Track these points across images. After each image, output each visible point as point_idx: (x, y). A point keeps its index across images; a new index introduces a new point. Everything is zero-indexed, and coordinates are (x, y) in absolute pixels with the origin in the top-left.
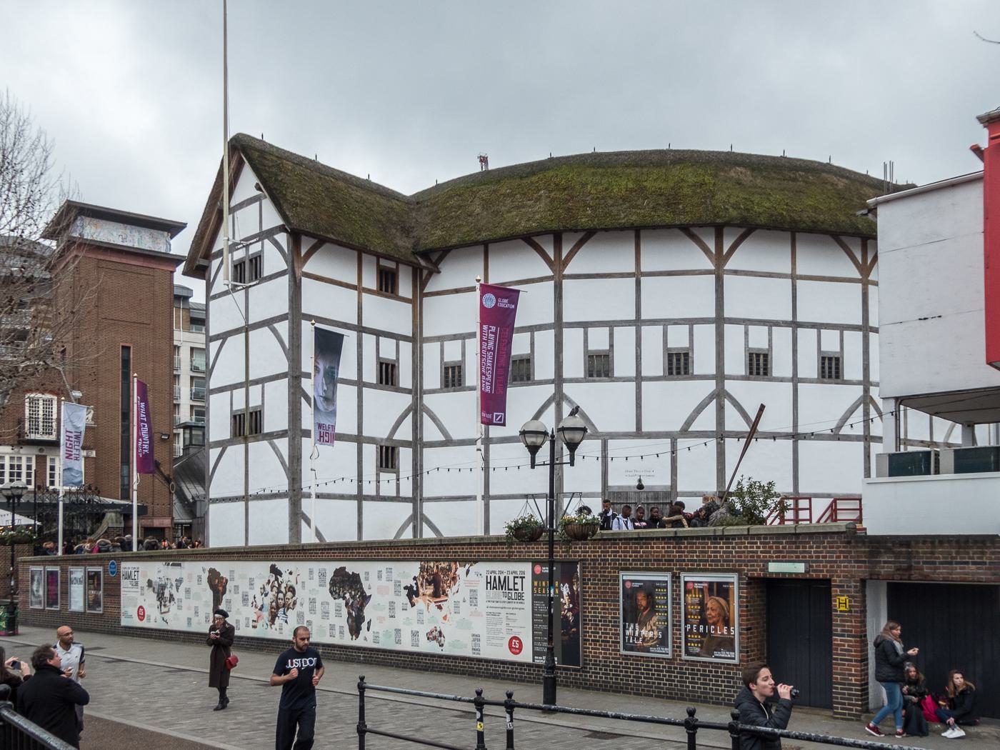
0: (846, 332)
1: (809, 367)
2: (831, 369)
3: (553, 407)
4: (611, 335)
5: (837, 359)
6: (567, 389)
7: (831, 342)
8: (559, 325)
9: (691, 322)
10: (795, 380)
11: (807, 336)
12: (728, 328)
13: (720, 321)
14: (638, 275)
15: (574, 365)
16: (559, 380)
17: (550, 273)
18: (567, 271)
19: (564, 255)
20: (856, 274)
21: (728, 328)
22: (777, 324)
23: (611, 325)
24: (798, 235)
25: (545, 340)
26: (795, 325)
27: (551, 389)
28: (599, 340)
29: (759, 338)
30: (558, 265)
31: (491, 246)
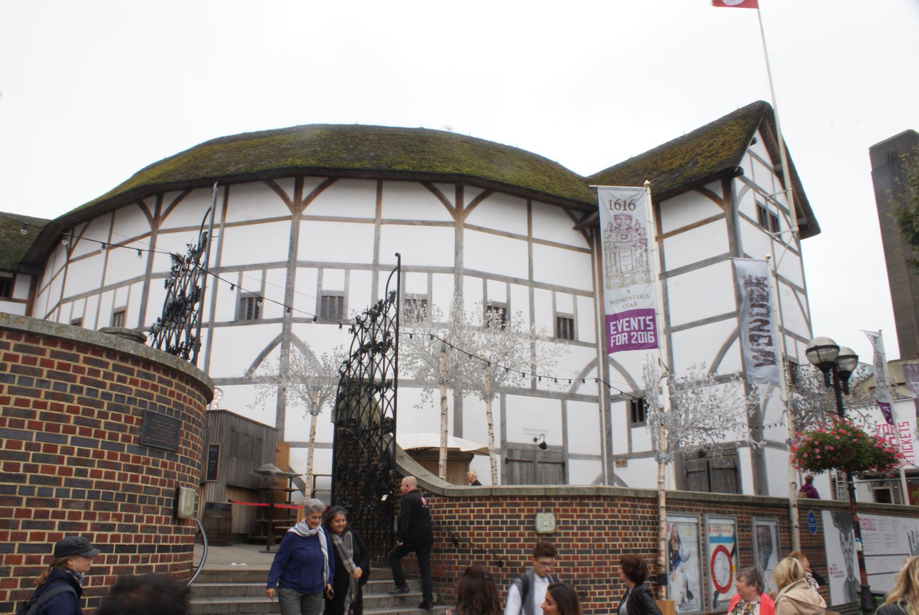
0: (578, 297)
1: (546, 325)
2: (565, 328)
3: (278, 350)
4: (347, 275)
5: (571, 321)
6: (296, 329)
7: (565, 306)
8: (292, 264)
9: (430, 271)
10: (533, 337)
11: (543, 297)
12: (466, 279)
13: (458, 271)
14: (378, 221)
15: (305, 305)
16: (287, 320)
17: (288, 212)
18: (307, 211)
19: (306, 193)
20: (587, 246)
21: (466, 279)
22: (517, 281)
23: (347, 267)
24: (533, 203)
25: (278, 277)
26: (532, 284)
27: (278, 329)
28: (333, 282)
29: (497, 292)
30: (297, 206)
31: (232, 188)
